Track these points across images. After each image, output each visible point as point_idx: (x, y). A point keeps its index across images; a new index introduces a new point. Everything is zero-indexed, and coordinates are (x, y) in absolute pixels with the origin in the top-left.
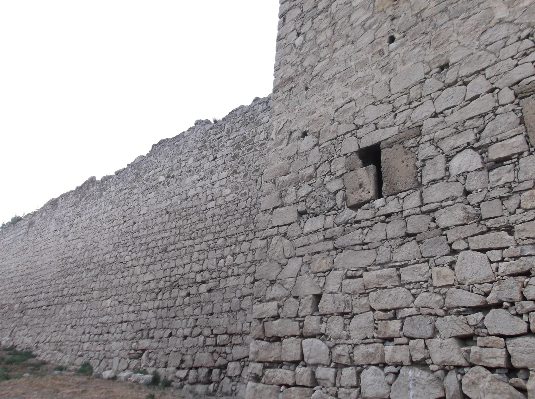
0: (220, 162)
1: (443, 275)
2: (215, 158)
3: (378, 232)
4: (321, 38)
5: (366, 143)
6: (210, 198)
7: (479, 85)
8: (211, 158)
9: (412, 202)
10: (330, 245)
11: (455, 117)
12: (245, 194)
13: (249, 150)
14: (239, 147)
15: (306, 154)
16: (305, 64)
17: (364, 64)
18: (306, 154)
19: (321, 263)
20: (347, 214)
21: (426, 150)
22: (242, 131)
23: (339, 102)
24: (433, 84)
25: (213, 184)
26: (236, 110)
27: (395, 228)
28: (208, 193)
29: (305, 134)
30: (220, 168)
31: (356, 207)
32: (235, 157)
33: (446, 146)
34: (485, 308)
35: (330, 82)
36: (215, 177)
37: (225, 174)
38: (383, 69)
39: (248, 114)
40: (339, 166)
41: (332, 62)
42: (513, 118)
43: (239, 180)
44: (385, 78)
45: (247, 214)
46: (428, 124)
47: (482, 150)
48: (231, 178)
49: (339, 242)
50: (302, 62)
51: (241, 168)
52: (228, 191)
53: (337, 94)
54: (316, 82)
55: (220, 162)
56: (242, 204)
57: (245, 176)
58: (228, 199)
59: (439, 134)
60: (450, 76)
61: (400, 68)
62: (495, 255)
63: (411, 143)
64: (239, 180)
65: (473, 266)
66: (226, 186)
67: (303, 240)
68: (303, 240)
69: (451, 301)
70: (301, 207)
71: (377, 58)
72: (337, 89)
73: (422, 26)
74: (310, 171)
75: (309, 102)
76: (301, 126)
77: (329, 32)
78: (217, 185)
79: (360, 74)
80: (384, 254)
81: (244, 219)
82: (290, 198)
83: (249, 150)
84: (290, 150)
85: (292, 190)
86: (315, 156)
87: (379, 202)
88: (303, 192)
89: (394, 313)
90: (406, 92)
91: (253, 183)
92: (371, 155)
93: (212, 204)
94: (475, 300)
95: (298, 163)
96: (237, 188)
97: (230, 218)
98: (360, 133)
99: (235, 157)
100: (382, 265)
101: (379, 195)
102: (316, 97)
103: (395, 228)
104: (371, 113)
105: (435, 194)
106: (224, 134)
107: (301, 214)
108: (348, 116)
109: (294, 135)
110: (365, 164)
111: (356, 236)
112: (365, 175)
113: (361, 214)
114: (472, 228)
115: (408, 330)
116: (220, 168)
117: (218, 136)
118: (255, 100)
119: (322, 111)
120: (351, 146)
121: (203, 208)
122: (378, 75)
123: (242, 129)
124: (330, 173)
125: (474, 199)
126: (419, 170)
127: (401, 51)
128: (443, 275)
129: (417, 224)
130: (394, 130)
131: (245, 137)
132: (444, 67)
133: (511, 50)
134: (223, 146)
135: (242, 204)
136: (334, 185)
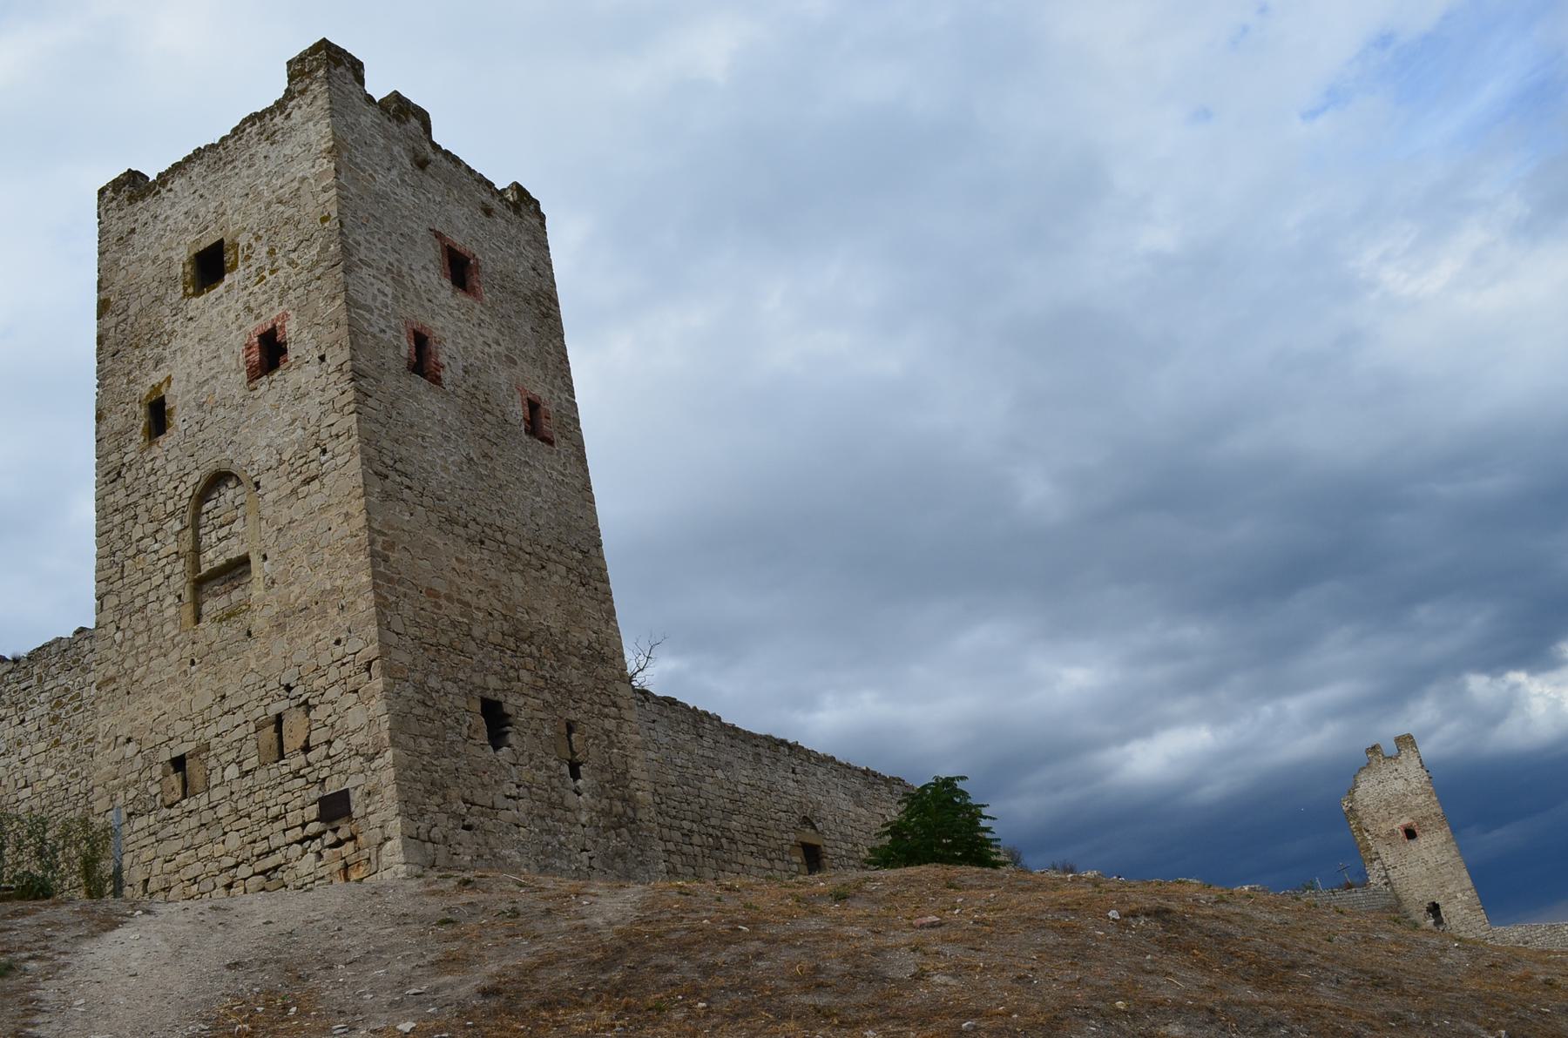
0: (31, 727)
1: (219, 849)
2: (23, 721)
3: (186, 824)
4: (139, 641)
5: (176, 754)
6: (21, 783)
7: (239, 717)
8: (16, 721)
9: (204, 801)
10: (153, 839)
11: (227, 739)
12: (77, 774)
13: (76, 709)
14: (59, 704)
15: (131, 760)
16: (126, 666)
17: (173, 680)
18: (131, 760)
19: (147, 854)
20: (165, 812)
21: (212, 762)
22: (62, 679)
23: (156, 713)
24: (217, 710)
25: (24, 761)
26: (50, 645)
27: (194, 822)
28: (17, 776)
29: (129, 740)
30: (33, 737)
31: (170, 806)
32: (55, 720)
33: (223, 759)
34: (237, 866)
35: (149, 690)
36: (25, 751)
37: (42, 746)
38: (188, 689)
39: (70, 653)
40: (157, 772)
41: (149, 671)
42: (254, 743)
43: (66, 754)
44: (188, 697)
45: (82, 802)
46: (214, 741)
47: (240, 764)
48: (53, 752)
49: (161, 835)
50: (123, 660)
51: (67, 736)
52: (50, 771)
53: (154, 705)
54: (135, 688)
55: (31, 727)
56: (74, 789)
57: (74, 747)
58: (51, 783)
59: (219, 751)
60: (226, 706)
61: (198, 692)
62: (242, 833)
63: (203, 756)
64: (66, 754)
65: (233, 841)
66: (45, 764)
67: (134, 837)
68: (134, 837)
69: (223, 865)
70: (130, 810)
71: (183, 678)
72: (154, 699)
73: (211, 656)
74: (135, 776)
75: (131, 708)
76: (125, 732)
77: (145, 635)
78: (31, 763)
79: (171, 690)
80: (188, 841)
81: (79, 810)
82: (120, 802)
83: (76, 709)
84: (117, 754)
85: (121, 793)
86: (139, 762)
87: (184, 802)
88: (130, 796)
89: (194, 880)
90: (201, 712)
91: (87, 757)
92: (179, 763)
93: (28, 791)
94: (232, 861)
95: (126, 767)
96: (63, 766)
97: (57, 810)
98: (171, 744)
99: (55, 720)
100: (187, 849)
101: (184, 797)
102: (137, 704)
103: (194, 822)
104: (180, 727)
105: (217, 794)
106: (34, 681)
107: (130, 815)
108: (162, 728)
109: (121, 740)
110: (176, 771)
111: (171, 829)
112: (175, 780)
113: (174, 812)
114: (233, 818)
115: (202, 889)
116: (33, 737)
117: (23, 686)
118: (77, 632)
119: (142, 719)
120: (165, 755)
121: (13, 799)
122: (183, 692)
123: (62, 676)
124: (151, 778)
125: (235, 797)
126: (207, 778)
127: (199, 675)
128: (219, 849)
129: (207, 816)
130: (192, 746)
131: (67, 690)
132: (223, 697)
133: (255, 695)
134: (34, 702)
135: (74, 789)
136: (155, 789)
